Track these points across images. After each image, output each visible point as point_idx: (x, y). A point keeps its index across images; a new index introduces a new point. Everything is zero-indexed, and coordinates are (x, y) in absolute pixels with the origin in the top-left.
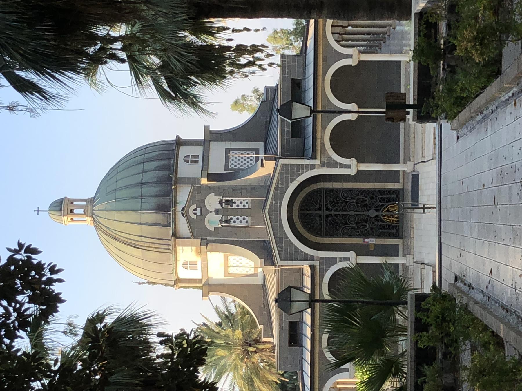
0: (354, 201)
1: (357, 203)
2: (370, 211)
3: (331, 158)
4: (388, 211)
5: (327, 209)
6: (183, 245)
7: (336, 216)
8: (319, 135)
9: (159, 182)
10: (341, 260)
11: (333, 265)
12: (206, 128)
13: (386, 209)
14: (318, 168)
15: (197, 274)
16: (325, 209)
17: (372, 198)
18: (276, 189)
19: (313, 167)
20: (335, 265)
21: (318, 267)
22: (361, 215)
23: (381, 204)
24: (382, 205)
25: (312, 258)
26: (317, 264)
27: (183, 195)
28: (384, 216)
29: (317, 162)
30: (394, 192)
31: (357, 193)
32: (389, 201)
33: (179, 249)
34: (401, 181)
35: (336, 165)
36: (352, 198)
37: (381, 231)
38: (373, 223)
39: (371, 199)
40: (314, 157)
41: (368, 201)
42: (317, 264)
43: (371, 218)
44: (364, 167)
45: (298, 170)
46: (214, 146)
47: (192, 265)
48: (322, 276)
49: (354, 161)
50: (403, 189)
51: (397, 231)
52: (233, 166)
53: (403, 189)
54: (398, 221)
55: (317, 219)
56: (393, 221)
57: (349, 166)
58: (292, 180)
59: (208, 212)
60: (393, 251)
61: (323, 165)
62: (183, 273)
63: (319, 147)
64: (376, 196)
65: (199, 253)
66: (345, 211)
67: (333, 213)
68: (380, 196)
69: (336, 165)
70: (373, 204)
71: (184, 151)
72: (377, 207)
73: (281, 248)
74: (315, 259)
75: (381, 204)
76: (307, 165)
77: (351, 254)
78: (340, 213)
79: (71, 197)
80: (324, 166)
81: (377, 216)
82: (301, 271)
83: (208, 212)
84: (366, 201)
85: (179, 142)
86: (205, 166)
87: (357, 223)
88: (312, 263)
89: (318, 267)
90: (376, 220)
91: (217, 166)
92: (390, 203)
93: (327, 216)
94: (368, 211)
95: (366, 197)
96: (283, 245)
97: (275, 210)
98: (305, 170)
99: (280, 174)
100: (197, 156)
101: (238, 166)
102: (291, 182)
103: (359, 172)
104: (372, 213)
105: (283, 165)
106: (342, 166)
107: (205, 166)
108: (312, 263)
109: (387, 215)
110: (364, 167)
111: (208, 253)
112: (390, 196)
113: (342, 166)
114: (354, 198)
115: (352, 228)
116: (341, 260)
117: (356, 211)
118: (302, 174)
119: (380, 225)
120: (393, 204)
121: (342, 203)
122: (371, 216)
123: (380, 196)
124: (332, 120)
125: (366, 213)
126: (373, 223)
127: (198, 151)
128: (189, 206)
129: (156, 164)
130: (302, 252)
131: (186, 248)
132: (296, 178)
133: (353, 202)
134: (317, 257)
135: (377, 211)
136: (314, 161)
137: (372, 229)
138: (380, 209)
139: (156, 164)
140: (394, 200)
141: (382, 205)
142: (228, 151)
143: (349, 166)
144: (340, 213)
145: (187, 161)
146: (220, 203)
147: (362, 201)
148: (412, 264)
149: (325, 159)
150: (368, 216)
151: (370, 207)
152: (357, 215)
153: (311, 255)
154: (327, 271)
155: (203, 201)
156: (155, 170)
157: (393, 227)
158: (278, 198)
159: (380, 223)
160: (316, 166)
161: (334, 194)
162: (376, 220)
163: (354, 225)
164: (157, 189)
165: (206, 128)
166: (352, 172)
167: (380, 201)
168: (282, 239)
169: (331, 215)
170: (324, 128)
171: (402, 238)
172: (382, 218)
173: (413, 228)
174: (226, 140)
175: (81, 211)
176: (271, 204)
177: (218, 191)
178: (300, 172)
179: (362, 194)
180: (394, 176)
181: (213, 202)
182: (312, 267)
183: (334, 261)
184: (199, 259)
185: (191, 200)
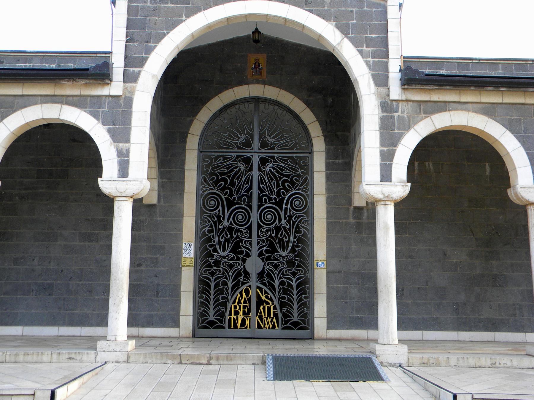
0: (283, 222)
1: (278, 229)
2: (259, 259)
3: (409, 128)
4: (260, 302)
5: (263, 161)
7: (249, 181)
8: (469, 97)
11: (109, 131)
13: (263, 298)
14: (378, 94)
16: (262, 155)
17: (290, 263)
19: (381, 80)
20: (107, 137)
21: (104, 91)
22: (250, 237)
23: (276, 284)
24: (272, 287)
25: (130, 78)
26: (116, 87)
28: (247, 292)
29: (396, 92)
30: (305, 315)
31: (302, 229)
32: (282, 305)
36: (290, 217)
37: (212, 285)
38: (231, 266)
39: (288, 262)
41: (284, 254)
43: (244, 261)
44: (386, 218)
48: (78, 102)
50: (312, 338)
51: (211, 324)
53: (312, 338)
54: (236, 327)
55: (242, 139)
56: (237, 313)
57: (386, 176)
58: (344, 30)
60: (150, 305)
61: (387, 107)
63: (437, 96)
64: (294, 274)
66: (260, 199)
67: (255, 174)
68: (294, 284)
70: (276, 267)
72: (269, 275)
74: (129, 85)
75: (276, 284)
78: (255, 191)
80: (382, 111)
81: (247, 275)
84: (284, 251)
87: (230, 229)
89: (104, 91)
90: (239, 274)
92: (278, 307)
93: (247, 161)
94: (260, 255)
95: (293, 250)
96: (169, 5)
98: (371, 60)
102: (337, 26)
103: (370, 209)
104: (254, 265)
106: (387, 159)
109: (249, 300)
110: (386, 218)
112: (295, 307)
113: (387, 159)
114: (289, 221)
115: (219, 217)
117: (259, 226)
118: (361, 52)
119: (225, 283)
120: (276, 315)
121: (278, 194)
122: (249, 261)
123: (294, 284)
124: (512, 131)
125: (254, 251)
126: (231, 266)
130: (149, 51)
132: (350, 39)
133: (280, 220)
134: (132, 92)
135: (261, 275)
136: (398, 83)
137: (217, 263)
138: (264, 284)
140: (285, 315)
141: (272, 287)
143: (386, 176)
144: (255, 191)
147: (281, 240)
148: (102, 356)
149: (404, 112)
150: (248, 255)
151: (268, 258)
152: (250, 228)
153: (139, 73)
154: (95, 115)
157: (222, 315)
159: (230, 284)
160: (383, 90)
161: (299, 176)
162: (239, 274)
163: (225, 222)
167: (282, 283)
169: (251, 169)
170: (489, 110)
171: (194, 336)
172: (245, 287)
173: (209, 363)
178: (364, 48)
179: (300, 240)
183: (120, 132)
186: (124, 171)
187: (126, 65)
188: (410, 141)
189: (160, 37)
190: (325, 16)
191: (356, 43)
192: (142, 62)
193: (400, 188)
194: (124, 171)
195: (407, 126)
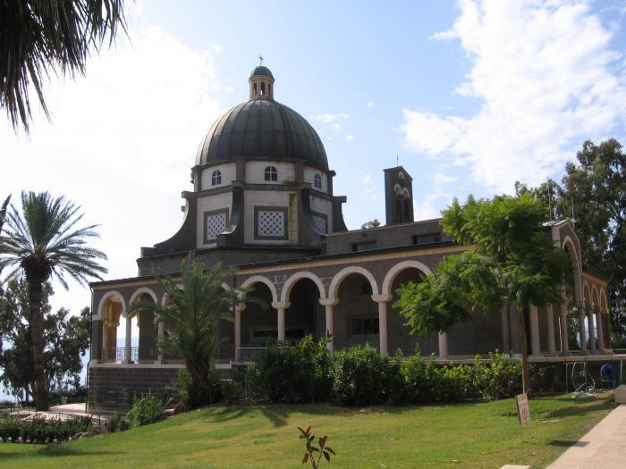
12: (344, 199)
46: (329, 205)
47: (217, 178)
100: (320, 187)
127: (324, 189)
142: (324, 217)
145: (316, 177)
165: (344, 199)
174: (333, 216)
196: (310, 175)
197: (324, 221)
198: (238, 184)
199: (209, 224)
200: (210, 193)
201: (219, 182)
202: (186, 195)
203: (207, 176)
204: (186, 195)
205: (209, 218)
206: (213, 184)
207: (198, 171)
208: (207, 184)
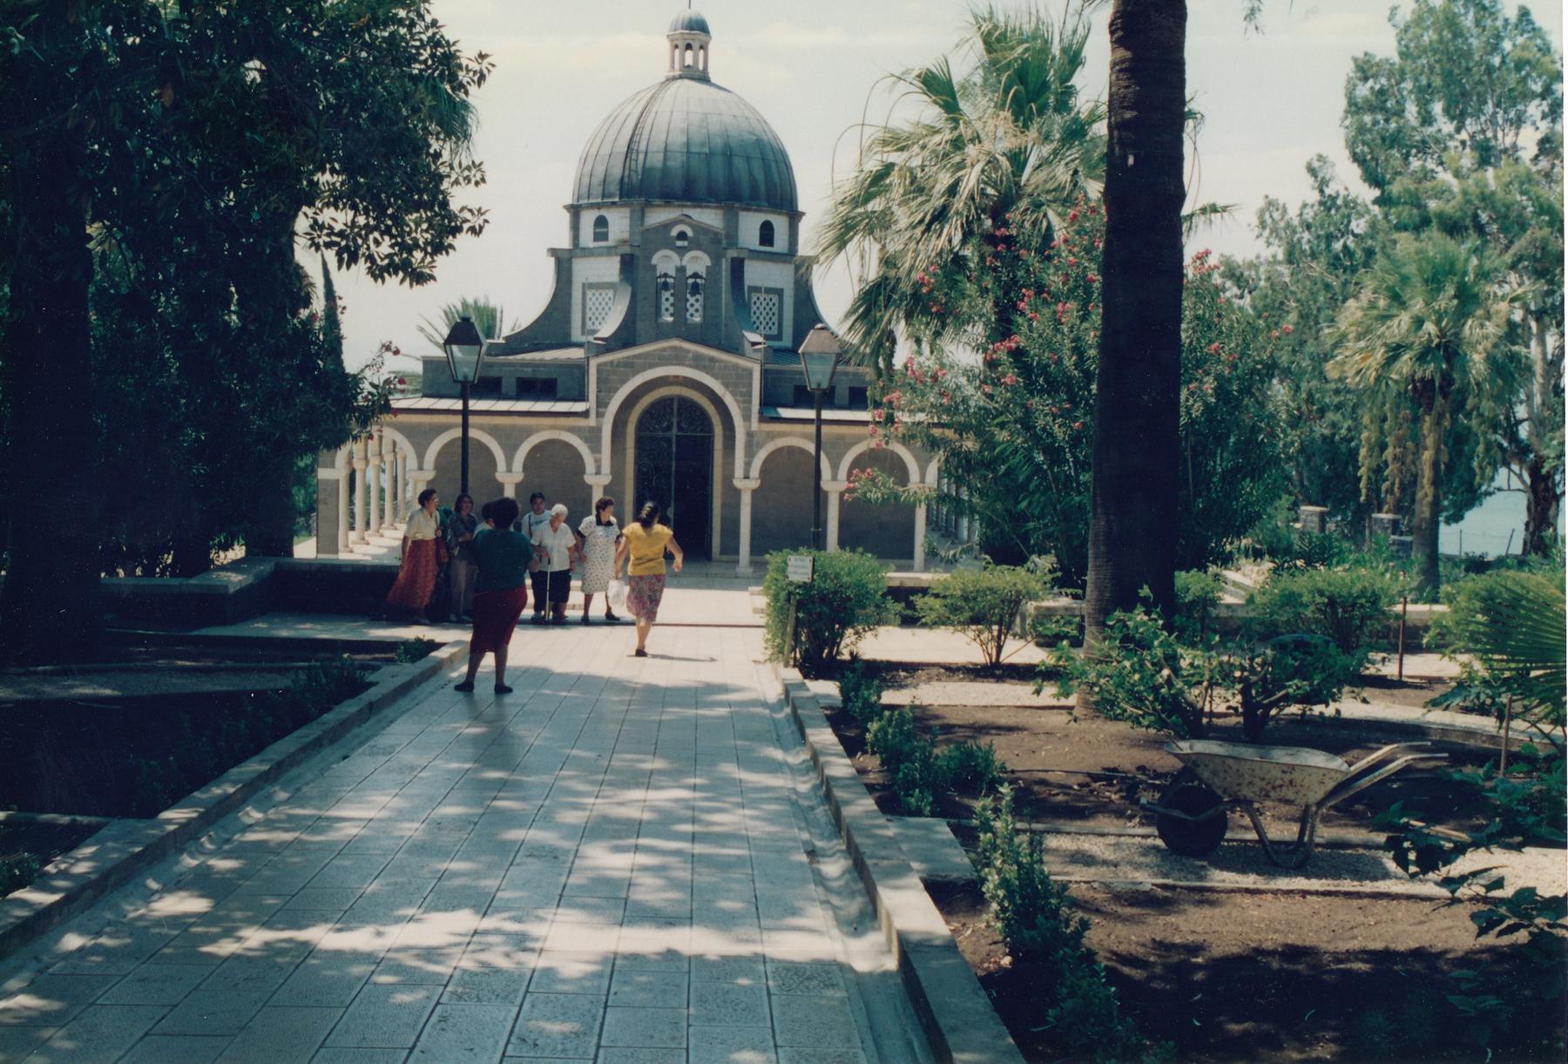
6: (631, 218)
9: (732, 183)
10: (598, 463)
15: (587, 239)
18: (712, 360)
19: (747, 417)
25: (600, 415)
26: (592, 421)
27: (710, 217)
33: (626, 212)
34: (725, 558)
35: (750, 453)
40: (762, 419)
42: (592, 421)
45: (742, 394)
47: (600, 236)
48: (571, 430)
49: (755, 484)
52: (754, 298)
57: (747, 477)
58: (726, 386)
59: (681, 256)
61: (750, 435)
62: (588, 219)
65: (624, 242)
69: (750, 453)
71: (780, 223)
73: (618, 365)
76: (750, 410)
77: (606, 479)
79: (711, 47)
82: (582, 397)
83: (681, 256)
85: (795, 216)
86: (755, 255)
88: (593, 414)
91: (755, 273)
97: (678, 358)
99: (736, 367)
100: (771, 244)
101: (754, 308)
105: (750, 372)
106: (748, 465)
107: (755, 255)
108: (593, 414)
111: (618, 259)
113: (748, 465)
116: (598, 463)
128: (690, 225)
129: (760, 177)
130: (610, 398)
131: (626, 222)
139: (760, 177)
142: (779, 292)
146: (696, 275)
155: (699, 248)
156: (751, 175)
158: (698, 362)
164: (721, 180)
166: (738, 483)
168: (632, 367)
175: (689, 60)
176: (688, 351)
177: (713, 271)
180: (731, 548)
181: (698, 262)
182: (585, 414)
184: (611, 242)
185: (699, 228)
186: (598, 472)
187: (598, 406)
188: (762, 455)
189: (617, 389)
190: (714, 376)
191: (734, 394)
192: (606, 405)
193: (754, 484)
194: (598, 472)
195: (760, 446)
196: (750, 225)
197: (775, 299)
198: (627, 250)
199: (589, 304)
200: (588, 253)
201: (604, 237)
202: (553, 252)
203: (588, 219)
204: (553, 252)
205: (589, 294)
206: (596, 239)
207: (575, 210)
208: (587, 239)
